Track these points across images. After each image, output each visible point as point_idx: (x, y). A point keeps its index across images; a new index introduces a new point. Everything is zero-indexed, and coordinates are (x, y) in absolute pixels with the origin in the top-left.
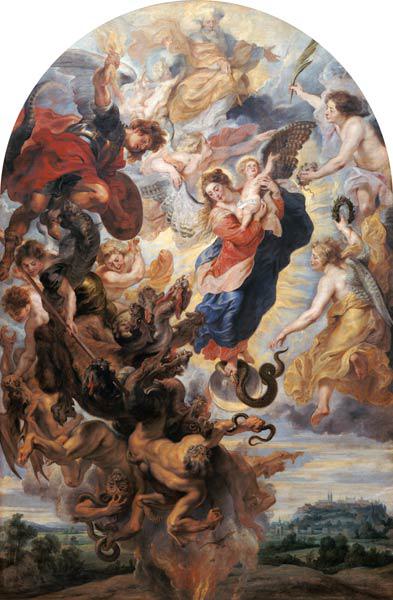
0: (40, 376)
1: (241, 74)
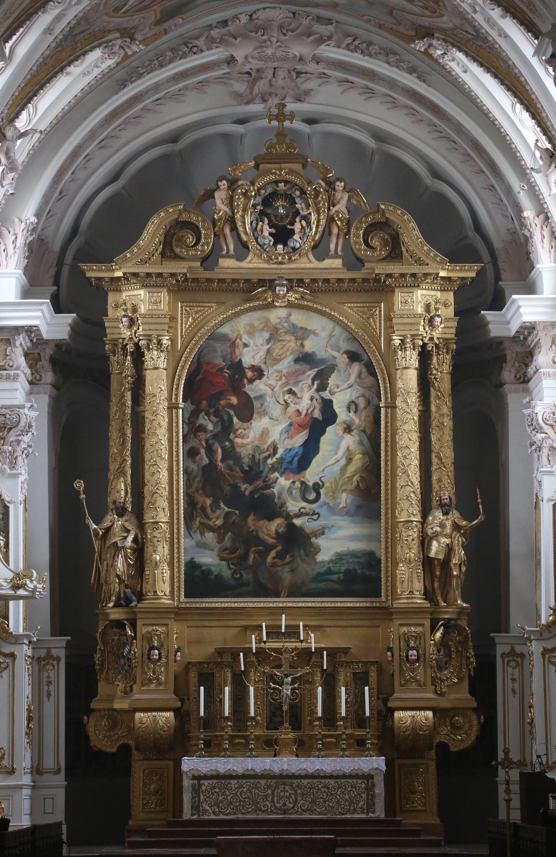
1: (301, 342)
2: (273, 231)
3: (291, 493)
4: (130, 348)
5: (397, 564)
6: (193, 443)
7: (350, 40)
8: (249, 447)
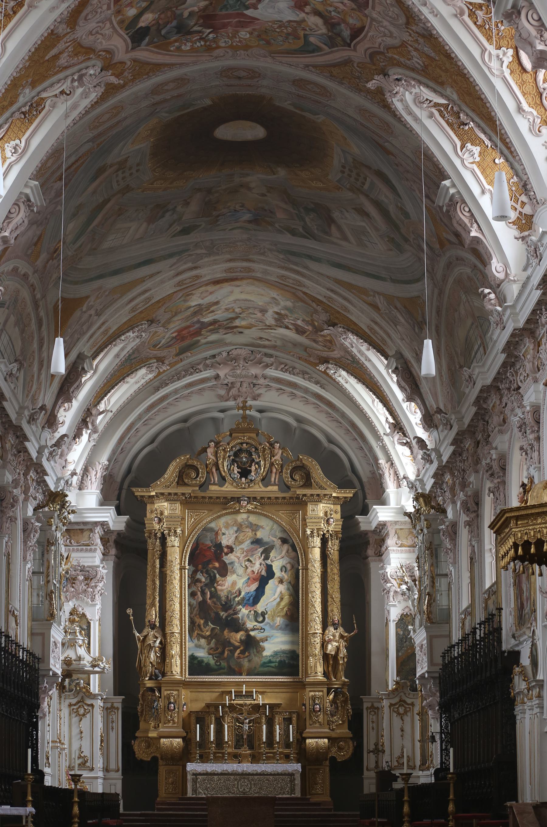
0: (199, 614)
2: (240, 470)
3: (249, 617)
4: (159, 535)
5: (308, 658)
6: (194, 589)
7: (283, 366)
8: (225, 591)
